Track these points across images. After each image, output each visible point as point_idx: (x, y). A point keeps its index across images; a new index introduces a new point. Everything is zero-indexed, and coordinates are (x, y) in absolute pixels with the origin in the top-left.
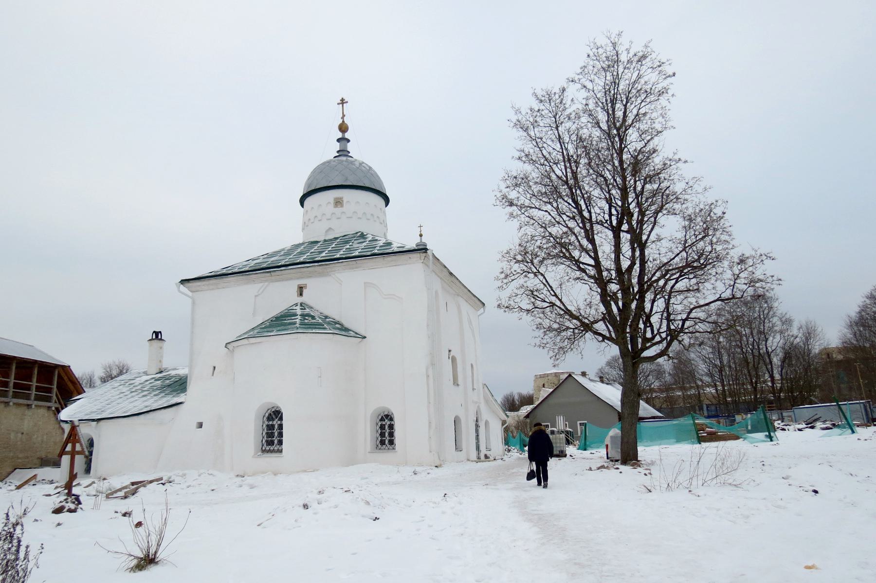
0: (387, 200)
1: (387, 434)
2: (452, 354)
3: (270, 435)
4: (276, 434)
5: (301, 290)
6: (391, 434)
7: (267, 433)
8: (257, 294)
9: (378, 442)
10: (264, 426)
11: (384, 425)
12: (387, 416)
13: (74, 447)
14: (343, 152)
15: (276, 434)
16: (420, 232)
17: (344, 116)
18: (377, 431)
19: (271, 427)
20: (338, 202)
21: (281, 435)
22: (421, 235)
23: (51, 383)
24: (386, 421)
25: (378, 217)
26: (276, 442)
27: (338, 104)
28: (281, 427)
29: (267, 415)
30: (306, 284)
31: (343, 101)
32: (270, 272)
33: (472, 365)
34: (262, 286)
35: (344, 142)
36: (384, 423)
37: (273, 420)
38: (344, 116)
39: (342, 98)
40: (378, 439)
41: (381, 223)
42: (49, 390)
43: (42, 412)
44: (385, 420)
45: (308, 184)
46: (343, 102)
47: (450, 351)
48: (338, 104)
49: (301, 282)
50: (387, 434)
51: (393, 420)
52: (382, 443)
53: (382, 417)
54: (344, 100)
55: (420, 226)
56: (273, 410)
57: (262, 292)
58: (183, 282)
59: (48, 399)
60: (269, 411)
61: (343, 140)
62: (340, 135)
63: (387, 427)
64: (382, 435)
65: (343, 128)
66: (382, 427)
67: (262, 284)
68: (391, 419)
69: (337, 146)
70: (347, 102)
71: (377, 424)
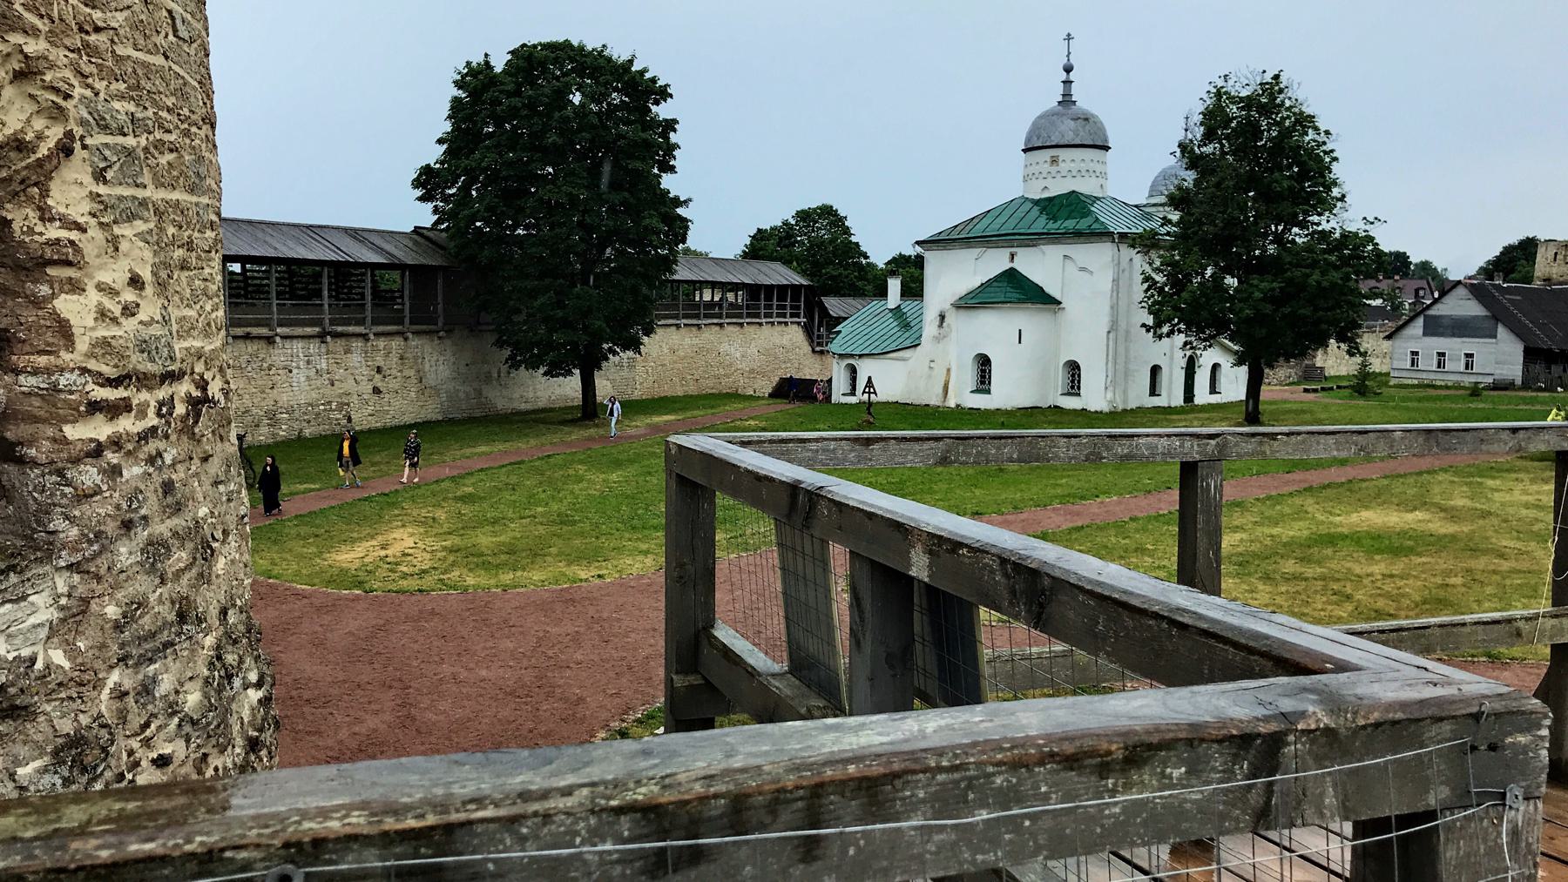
0: (1107, 148)
3: (983, 377)
5: (1012, 256)
6: (1079, 382)
17: (1069, 53)
19: (983, 371)
20: (1054, 161)
23: (800, 302)
28: (990, 371)
35: (1068, 85)
38: (1069, 53)
42: (798, 308)
43: (795, 327)
45: (1028, 140)
46: (1069, 37)
52: (1072, 387)
58: (918, 243)
61: (1067, 83)
62: (1064, 76)
64: (1073, 381)
65: (1068, 69)
66: (1073, 375)
68: (1079, 370)
69: (1060, 88)
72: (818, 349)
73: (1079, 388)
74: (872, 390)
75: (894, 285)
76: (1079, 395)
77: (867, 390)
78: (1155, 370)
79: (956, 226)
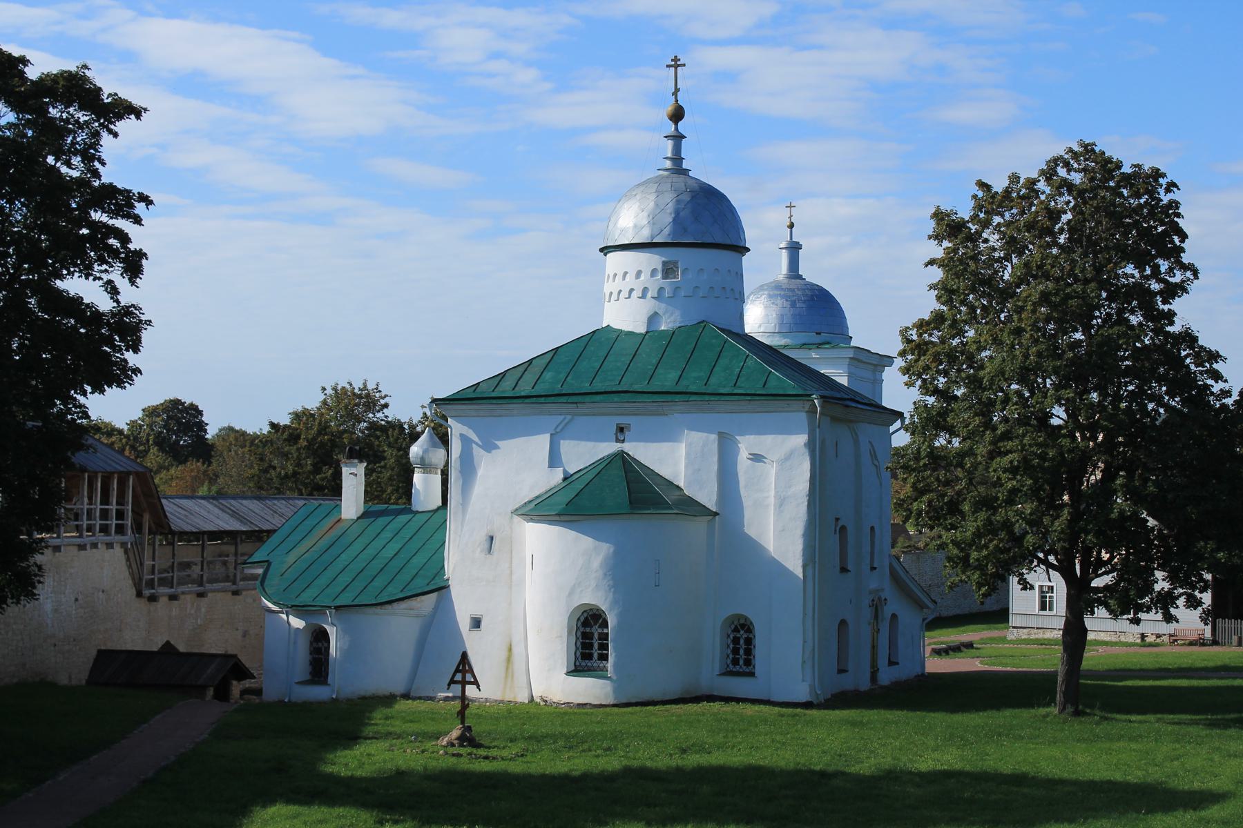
1: (742, 652)
2: (841, 523)
4: (596, 646)
5: (621, 429)
6: (749, 652)
7: (582, 643)
8: (553, 432)
9: (729, 661)
10: (579, 634)
11: (739, 638)
12: (743, 626)
13: (464, 677)
14: (677, 159)
15: (596, 646)
16: (790, 217)
17: (677, 90)
18: (728, 646)
21: (604, 647)
22: (791, 226)
24: (742, 632)
25: (732, 290)
26: (596, 656)
27: (668, 66)
28: (605, 637)
29: (582, 619)
30: (630, 425)
31: (676, 63)
32: (576, 403)
33: (872, 528)
34: (565, 419)
36: (738, 636)
37: (591, 627)
38: (677, 90)
39: (676, 57)
40: (728, 656)
41: (736, 299)
44: (739, 632)
47: (837, 519)
48: (668, 66)
49: (623, 420)
50: (742, 652)
51: (751, 632)
52: (735, 662)
53: (736, 626)
54: (679, 60)
55: (791, 207)
56: (591, 613)
57: (562, 430)
59: (120, 529)
60: (585, 615)
61: (678, 138)
63: (742, 641)
64: (735, 651)
65: (677, 115)
66: (736, 641)
67: (561, 418)
70: (684, 65)
71: (729, 636)
72: (147, 592)
73: (748, 662)
74: (469, 678)
75: (353, 479)
76: (752, 674)
77: (459, 677)
78: (843, 623)
79: (504, 374)
